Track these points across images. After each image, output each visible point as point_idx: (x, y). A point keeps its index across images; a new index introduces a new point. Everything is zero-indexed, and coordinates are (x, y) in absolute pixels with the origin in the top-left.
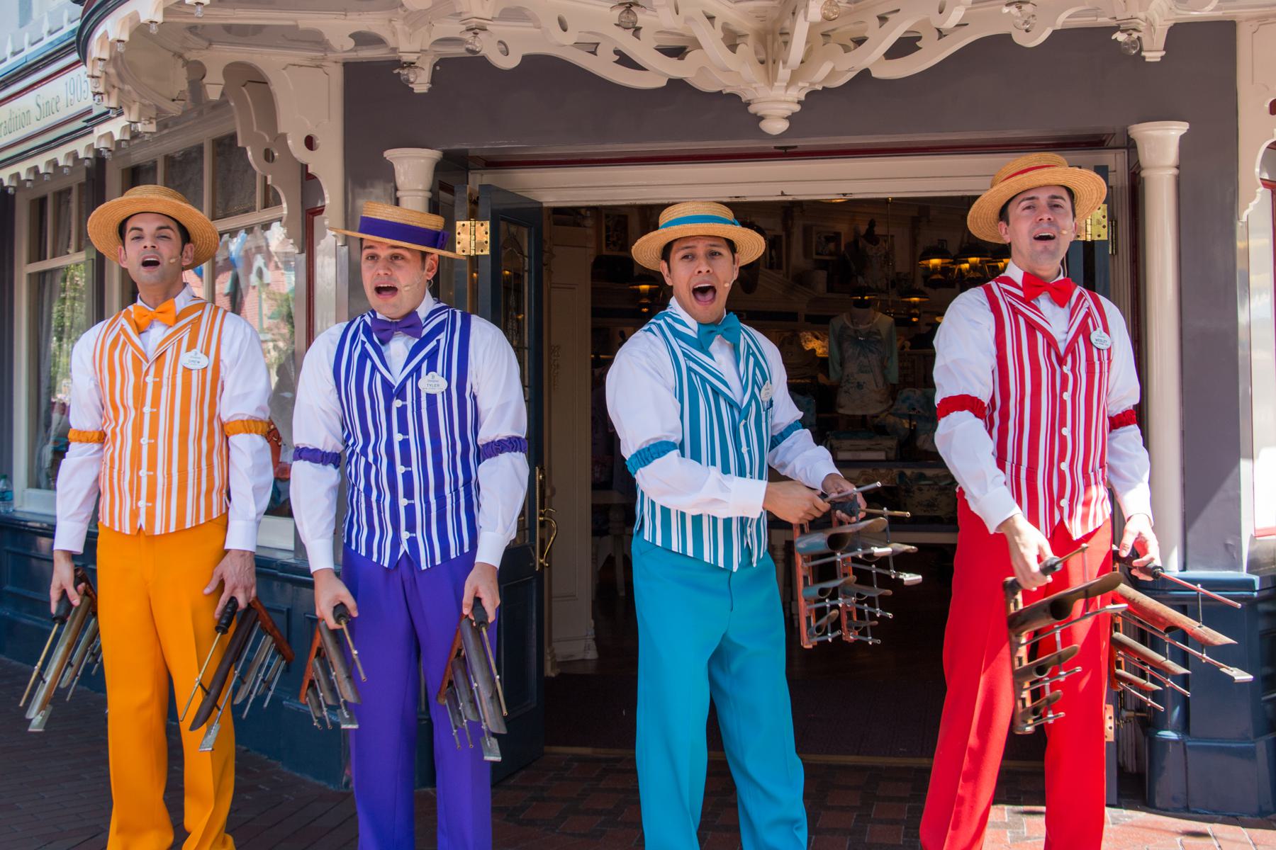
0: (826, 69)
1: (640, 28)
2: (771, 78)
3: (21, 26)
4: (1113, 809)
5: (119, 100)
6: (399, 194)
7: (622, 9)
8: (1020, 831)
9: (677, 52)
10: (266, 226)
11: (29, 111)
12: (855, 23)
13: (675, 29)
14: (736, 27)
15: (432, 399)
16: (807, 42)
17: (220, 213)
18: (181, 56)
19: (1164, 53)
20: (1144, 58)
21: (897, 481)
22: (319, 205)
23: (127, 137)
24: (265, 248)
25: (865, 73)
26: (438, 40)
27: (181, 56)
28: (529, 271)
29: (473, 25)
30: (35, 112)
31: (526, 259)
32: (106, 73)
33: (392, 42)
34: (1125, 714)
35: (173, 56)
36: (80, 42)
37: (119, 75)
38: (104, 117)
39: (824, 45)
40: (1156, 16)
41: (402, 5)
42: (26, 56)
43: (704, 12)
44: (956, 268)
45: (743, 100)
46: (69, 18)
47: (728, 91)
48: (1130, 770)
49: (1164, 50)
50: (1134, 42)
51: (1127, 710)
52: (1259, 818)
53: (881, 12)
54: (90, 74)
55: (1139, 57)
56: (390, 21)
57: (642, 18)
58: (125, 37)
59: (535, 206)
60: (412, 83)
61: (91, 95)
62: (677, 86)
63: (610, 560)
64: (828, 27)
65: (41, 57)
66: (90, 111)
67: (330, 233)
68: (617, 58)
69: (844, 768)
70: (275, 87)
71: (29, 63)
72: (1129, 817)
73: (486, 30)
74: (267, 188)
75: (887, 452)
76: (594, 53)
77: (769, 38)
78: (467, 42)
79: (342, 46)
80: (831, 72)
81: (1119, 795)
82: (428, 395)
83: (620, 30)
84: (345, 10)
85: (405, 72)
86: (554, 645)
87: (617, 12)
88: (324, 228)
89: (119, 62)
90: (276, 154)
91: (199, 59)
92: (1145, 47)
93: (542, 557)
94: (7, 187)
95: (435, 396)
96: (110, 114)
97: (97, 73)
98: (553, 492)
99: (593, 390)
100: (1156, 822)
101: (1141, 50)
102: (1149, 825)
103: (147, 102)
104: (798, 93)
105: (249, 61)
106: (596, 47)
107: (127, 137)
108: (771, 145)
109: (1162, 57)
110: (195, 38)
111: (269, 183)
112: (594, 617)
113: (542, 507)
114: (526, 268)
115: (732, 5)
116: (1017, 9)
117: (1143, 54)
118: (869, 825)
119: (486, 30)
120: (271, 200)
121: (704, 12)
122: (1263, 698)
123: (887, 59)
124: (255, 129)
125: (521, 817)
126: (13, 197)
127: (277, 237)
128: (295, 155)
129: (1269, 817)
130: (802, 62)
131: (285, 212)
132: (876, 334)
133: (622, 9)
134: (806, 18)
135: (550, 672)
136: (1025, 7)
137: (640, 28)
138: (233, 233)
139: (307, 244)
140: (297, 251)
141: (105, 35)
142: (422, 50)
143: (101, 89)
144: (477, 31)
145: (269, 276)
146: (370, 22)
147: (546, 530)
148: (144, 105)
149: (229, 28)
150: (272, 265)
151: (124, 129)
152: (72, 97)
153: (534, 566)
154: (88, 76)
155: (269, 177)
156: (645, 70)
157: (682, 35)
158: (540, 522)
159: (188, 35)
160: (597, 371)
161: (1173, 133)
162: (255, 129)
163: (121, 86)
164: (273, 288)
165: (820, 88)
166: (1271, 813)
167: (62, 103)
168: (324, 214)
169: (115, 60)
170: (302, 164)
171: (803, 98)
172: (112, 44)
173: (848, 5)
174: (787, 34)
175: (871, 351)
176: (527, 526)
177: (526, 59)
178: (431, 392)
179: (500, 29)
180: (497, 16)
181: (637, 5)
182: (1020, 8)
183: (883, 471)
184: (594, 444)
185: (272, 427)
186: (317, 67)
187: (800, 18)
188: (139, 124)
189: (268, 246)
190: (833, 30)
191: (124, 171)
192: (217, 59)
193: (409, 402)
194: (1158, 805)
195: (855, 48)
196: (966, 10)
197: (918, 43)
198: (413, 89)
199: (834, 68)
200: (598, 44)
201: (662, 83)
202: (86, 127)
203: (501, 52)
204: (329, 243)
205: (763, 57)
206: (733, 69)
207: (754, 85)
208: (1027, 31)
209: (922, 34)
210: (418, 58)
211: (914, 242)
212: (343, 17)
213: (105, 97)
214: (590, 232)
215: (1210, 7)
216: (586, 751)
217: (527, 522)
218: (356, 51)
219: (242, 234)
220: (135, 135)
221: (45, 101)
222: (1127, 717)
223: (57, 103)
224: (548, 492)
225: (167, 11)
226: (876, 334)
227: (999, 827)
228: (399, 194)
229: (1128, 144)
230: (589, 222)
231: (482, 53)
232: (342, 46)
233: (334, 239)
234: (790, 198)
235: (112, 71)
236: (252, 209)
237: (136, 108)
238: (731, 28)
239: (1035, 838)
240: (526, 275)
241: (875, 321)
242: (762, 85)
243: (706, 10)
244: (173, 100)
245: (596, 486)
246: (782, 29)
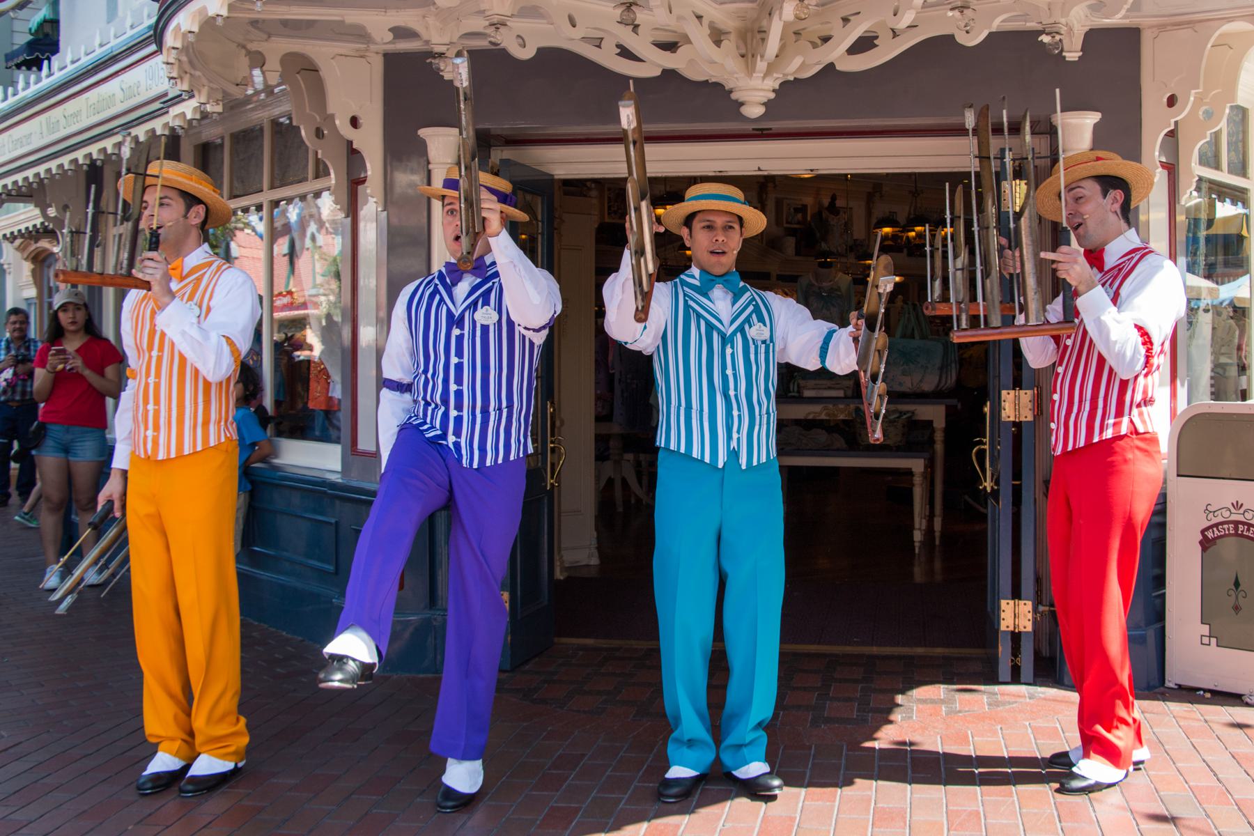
0: (797, 61)
1: (638, 25)
2: (750, 70)
3: (108, 23)
4: (1030, 687)
5: (191, 85)
6: (431, 167)
7: (624, 8)
8: (953, 706)
9: (670, 47)
10: (317, 195)
11: (114, 95)
12: (822, 24)
13: (669, 26)
14: (722, 26)
15: (485, 328)
16: (781, 39)
17: (277, 183)
18: (244, 47)
19: (1081, 54)
20: (1064, 57)
21: (854, 415)
22: (362, 176)
23: (198, 116)
24: (317, 216)
25: (831, 66)
26: (466, 34)
27: (244, 47)
28: (542, 234)
29: (495, 21)
30: (120, 95)
31: (540, 224)
32: (179, 60)
33: (425, 35)
34: (1041, 608)
35: (238, 46)
36: (157, 35)
37: (191, 62)
38: (177, 100)
39: (796, 42)
40: (1075, 22)
41: (434, 3)
42: (112, 47)
43: (694, 12)
44: (905, 235)
45: (726, 88)
46: (148, 15)
47: (714, 80)
48: (1044, 654)
49: (1082, 50)
50: (1056, 43)
51: (1043, 605)
52: (1146, 692)
53: (843, 15)
54: (165, 61)
55: (1060, 57)
56: (424, 17)
57: (641, 16)
58: (196, 29)
59: (547, 178)
60: (442, 71)
61: (167, 79)
62: (670, 75)
63: (610, 481)
64: (802, 25)
65: (125, 48)
66: (166, 94)
67: (372, 200)
68: (619, 50)
69: (809, 655)
70: (324, 73)
71: (115, 53)
72: (1043, 693)
73: (506, 25)
74: (318, 161)
75: (845, 391)
76: (599, 46)
77: (749, 35)
78: (490, 36)
79: (382, 39)
80: (801, 65)
81: (1036, 675)
82: (482, 326)
83: (622, 26)
84: (385, 8)
85: (436, 61)
86: (563, 552)
87: (619, 11)
88: (367, 196)
89: (191, 50)
90: (325, 132)
91: (260, 50)
92: (1066, 48)
93: (552, 478)
94: (96, 160)
95: (488, 326)
96: (183, 97)
97: (171, 60)
98: (562, 423)
99: (596, 336)
100: (1064, 697)
101: (1062, 51)
102: (1059, 699)
103: (215, 86)
104: (773, 83)
105: (304, 52)
106: (600, 43)
107: (198, 116)
108: (749, 127)
109: (1079, 57)
110: (256, 31)
111: (319, 156)
112: (597, 529)
113: (553, 435)
114: (540, 231)
115: (717, 6)
116: (959, 14)
117: (1064, 54)
118: (828, 702)
119: (506, 25)
120: (321, 171)
121: (694, 12)
122: (1154, 594)
123: (849, 54)
124: (308, 111)
125: (535, 697)
126: (101, 168)
127: (327, 206)
128: (342, 133)
129: (1157, 690)
130: (777, 56)
131: (333, 182)
132: (836, 290)
133: (624, 8)
134: (780, 19)
135: (559, 575)
136: (966, 11)
137: (638, 25)
138: (290, 200)
139: (352, 208)
140: (343, 215)
141: (178, 27)
142: (451, 43)
143: (174, 75)
144: (499, 26)
145: (321, 239)
146: (406, 18)
147: (556, 456)
148: (212, 88)
149: (285, 23)
150: (324, 231)
151: (195, 109)
152: (150, 82)
153: (546, 486)
154: (164, 63)
155: (320, 152)
156: (644, 61)
157: (675, 32)
158: (551, 448)
159: (251, 28)
160: (599, 320)
161: (1088, 121)
162: (308, 111)
163: (193, 72)
164: (325, 249)
165: (792, 78)
166: (1156, 688)
167: (143, 88)
168: (366, 184)
169: (186, 49)
170: (348, 141)
171: (777, 87)
172: (184, 35)
173: (816, 8)
174: (765, 32)
175: (833, 305)
176: (540, 451)
177: (541, 51)
178: (485, 323)
179: (518, 25)
180: (516, 13)
181: (637, 5)
182: (962, 12)
183: (841, 406)
184: (597, 383)
185: (322, 367)
186: (361, 57)
187: (776, 18)
188: (208, 105)
189: (320, 214)
190: (804, 29)
191: (196, 147)
192: (277, 48)
193: (466, 332)
194: (1066, 683)
195: (822, 45)
196: (917, 13)
197: (875, 42)
198: (443, 76)
199: (803, 62)
200: (602, 39)
201: (657, 72)
202: (162, 108)
203: (520, 45)
204: (371, 209)
205: (743, 51)
206: (716, 61)
207: (735, 76)
208: (967, 32)
209: (879, 34)
210: (448, 50)
211: (869, 214)
212: (383, 13)
213: (178, 81)
214: (595, 201)
215: (1123, 12)
216: (589, 642)
217: (540, 447)
218: (394, 43)
219: (297, 200)
220: (205, 115)
221: (128, 86)
222: (1042, 612)
223: (138, 87)
224: (558, 423)
225: (231, 7)
226: (836, 290)
227: (936, 703)
228: (431, 167)
229: (1051, 129)
230: (594, 193)
231: (502, 46)
232: (382, 39)
233: (375, 205)
234: (766, 173)
235: (184, 59)
236: (305, 179)
237: (205, 91)
238: (716, 26)
239: (966, 711)
240: (540, 237)
241: (836, 279)
242: (743, 75)
243: (695, 10)
244: (237, 85)
245: (599, 419)
246: (760, 27)
